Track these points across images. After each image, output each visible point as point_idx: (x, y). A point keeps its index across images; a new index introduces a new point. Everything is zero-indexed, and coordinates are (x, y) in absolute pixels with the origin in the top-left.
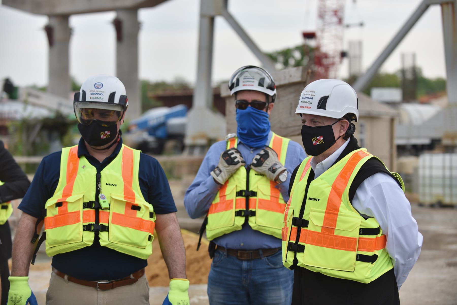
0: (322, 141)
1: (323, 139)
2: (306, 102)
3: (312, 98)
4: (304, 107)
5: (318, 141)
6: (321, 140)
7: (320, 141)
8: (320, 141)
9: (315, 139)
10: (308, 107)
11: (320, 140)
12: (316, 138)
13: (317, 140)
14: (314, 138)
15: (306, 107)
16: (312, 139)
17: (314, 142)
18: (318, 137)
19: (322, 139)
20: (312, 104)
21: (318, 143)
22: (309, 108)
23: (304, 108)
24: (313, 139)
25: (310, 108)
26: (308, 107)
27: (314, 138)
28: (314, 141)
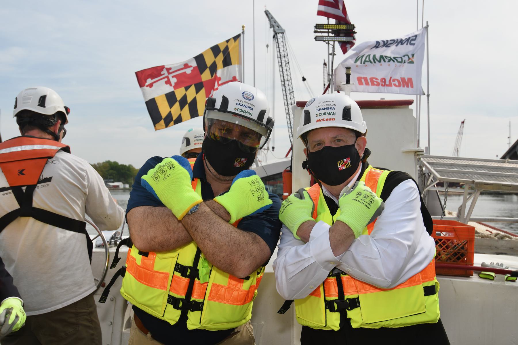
0: (350, 164)
1: (350, 161)
2: (325, 114)
3: (334, 108)
4: (325, 120)
5: (345, 164)
6: (348, 163)
7: (347, 165)
8: (347, 165)
9: (341, 163)
10: (330, 119)
11: (347, 164)
12: (342, 161)
13: (344, 164)
14: (340, 161)
15: (328, 119)
16: (338, 163)
17: (339, 167)
18: (345, 160)
19: (349, 161)
20: (335, 114)
21: (345, 168)
22: (332, 120)
23: (324, 121)
24: (339, 162)
25: (334, 120)
26: (330, 119)
27: (340, 161)
28: (340, 165)
